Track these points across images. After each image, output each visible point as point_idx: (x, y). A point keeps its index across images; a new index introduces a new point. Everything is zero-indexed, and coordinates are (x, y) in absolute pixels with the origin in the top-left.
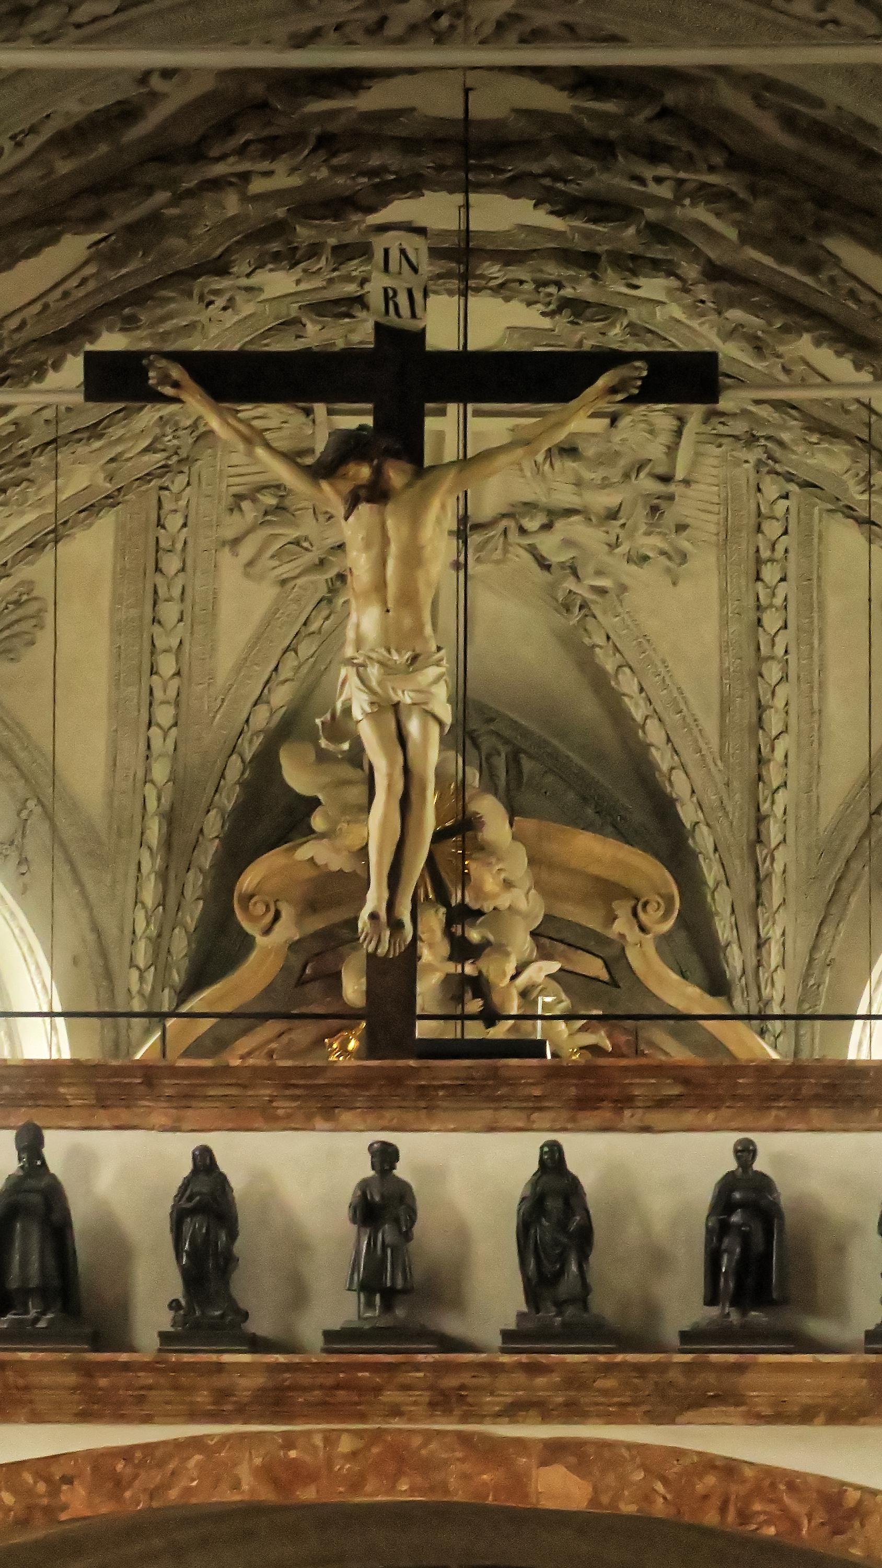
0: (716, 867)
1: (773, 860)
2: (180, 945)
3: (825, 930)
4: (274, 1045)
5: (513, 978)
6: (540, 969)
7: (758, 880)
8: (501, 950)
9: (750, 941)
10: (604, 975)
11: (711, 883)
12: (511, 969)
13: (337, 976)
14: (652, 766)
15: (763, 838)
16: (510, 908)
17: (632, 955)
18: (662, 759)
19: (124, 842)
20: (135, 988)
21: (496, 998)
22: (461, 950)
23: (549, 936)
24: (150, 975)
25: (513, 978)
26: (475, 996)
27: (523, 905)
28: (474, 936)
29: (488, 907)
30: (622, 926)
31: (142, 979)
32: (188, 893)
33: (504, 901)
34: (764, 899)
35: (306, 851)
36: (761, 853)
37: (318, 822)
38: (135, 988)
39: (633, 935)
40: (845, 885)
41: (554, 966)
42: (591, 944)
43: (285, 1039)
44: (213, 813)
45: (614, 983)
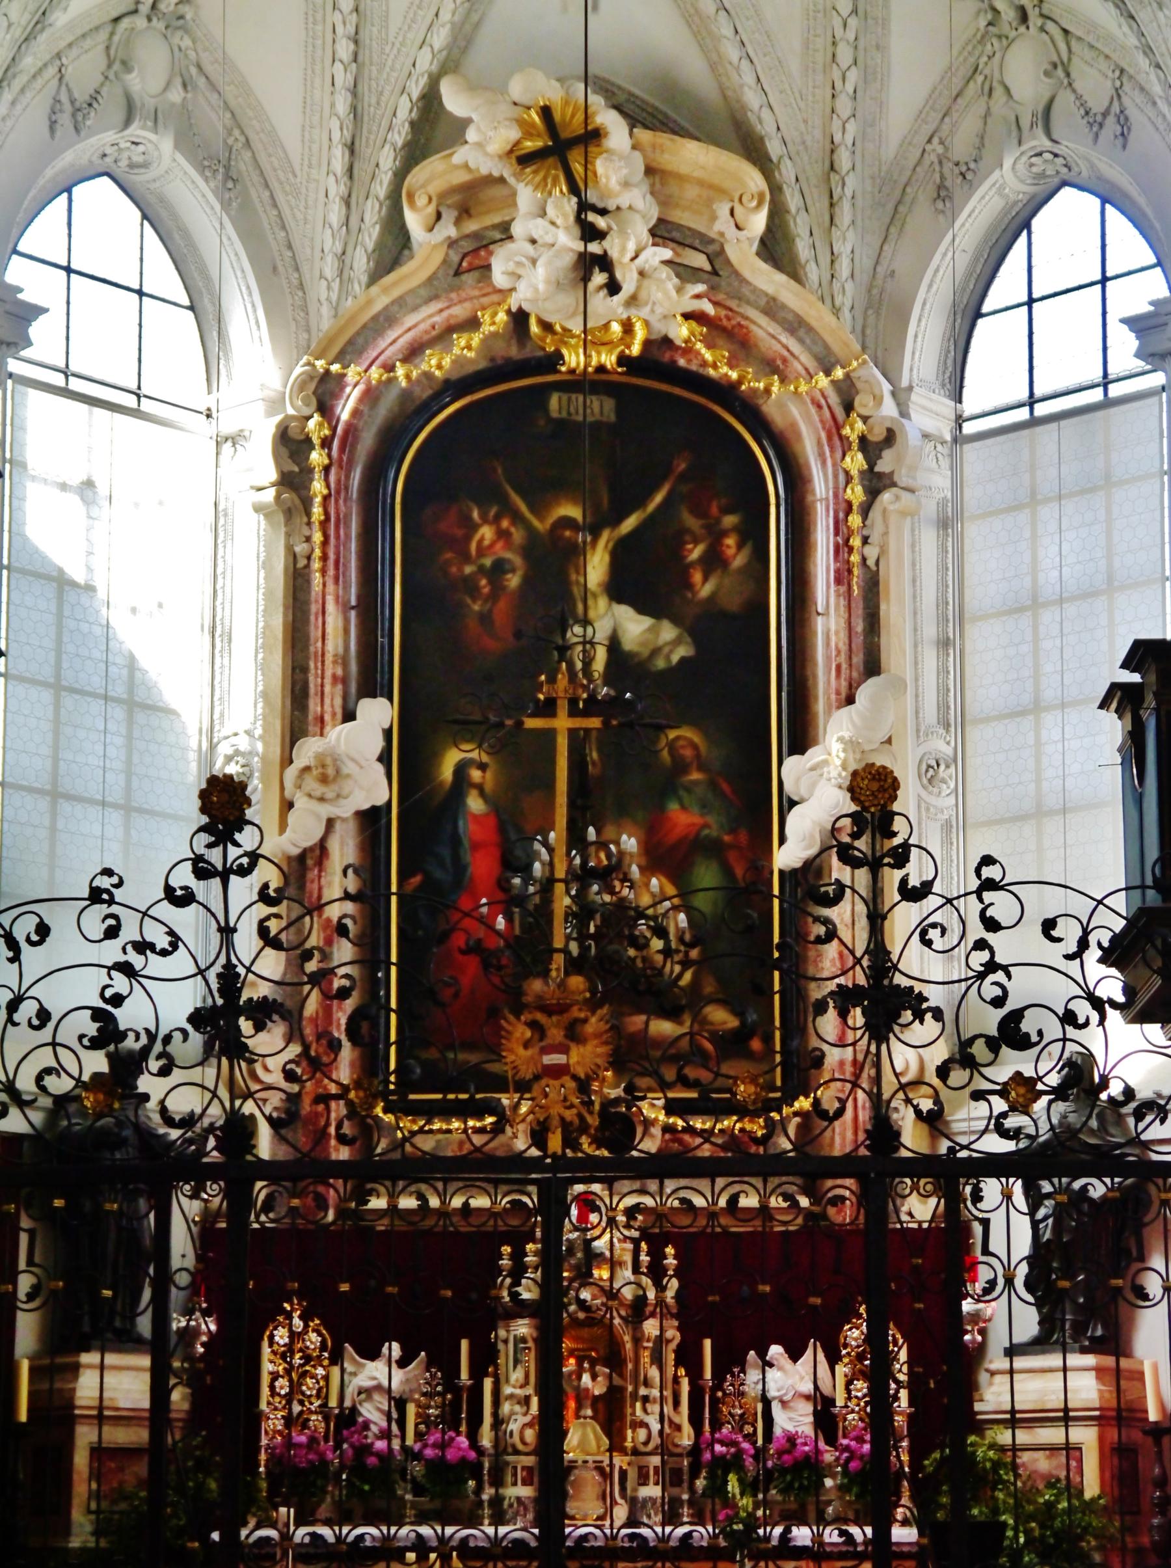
0: (797, 195)
1: (844, 184)
2: (361, 263)
3: (886, 248)
4: (437, 319)
5: (633, 259)
6: (655, 254)
7: (832, 205)
8: (623, 232)
9: (825, 259)
10: (708, 267)
11: (793, 210)
12: (631, 247)
13: (488, 267)
14: (744, 108)
15: (836, 166)
16: (630, 207)
17: (732, 253)
18: (752, 99)
19: (314, 171)
20: (323, 296)
21: (618, 275)
22: (590, 233)
23: (662, 232)
24: (336, 285)
25: (633, 259)
26: (601, 270)
27: (640, 204)
28: (601, 222)
29: (611, 206)
30: (723, 224)
31: (329, 288)
32: (367, 218)
33: (624, 200)
34: (837, 220)
35: (461, 155)
36: (834, 178)
37: (471, 135)
38: (323, 296)
39: (731, 232)
40: (901, 208)
41: (667, 254)
42: (697, 243)
43: (445, 314)
44: (387, 147)
45: (715, 273)
